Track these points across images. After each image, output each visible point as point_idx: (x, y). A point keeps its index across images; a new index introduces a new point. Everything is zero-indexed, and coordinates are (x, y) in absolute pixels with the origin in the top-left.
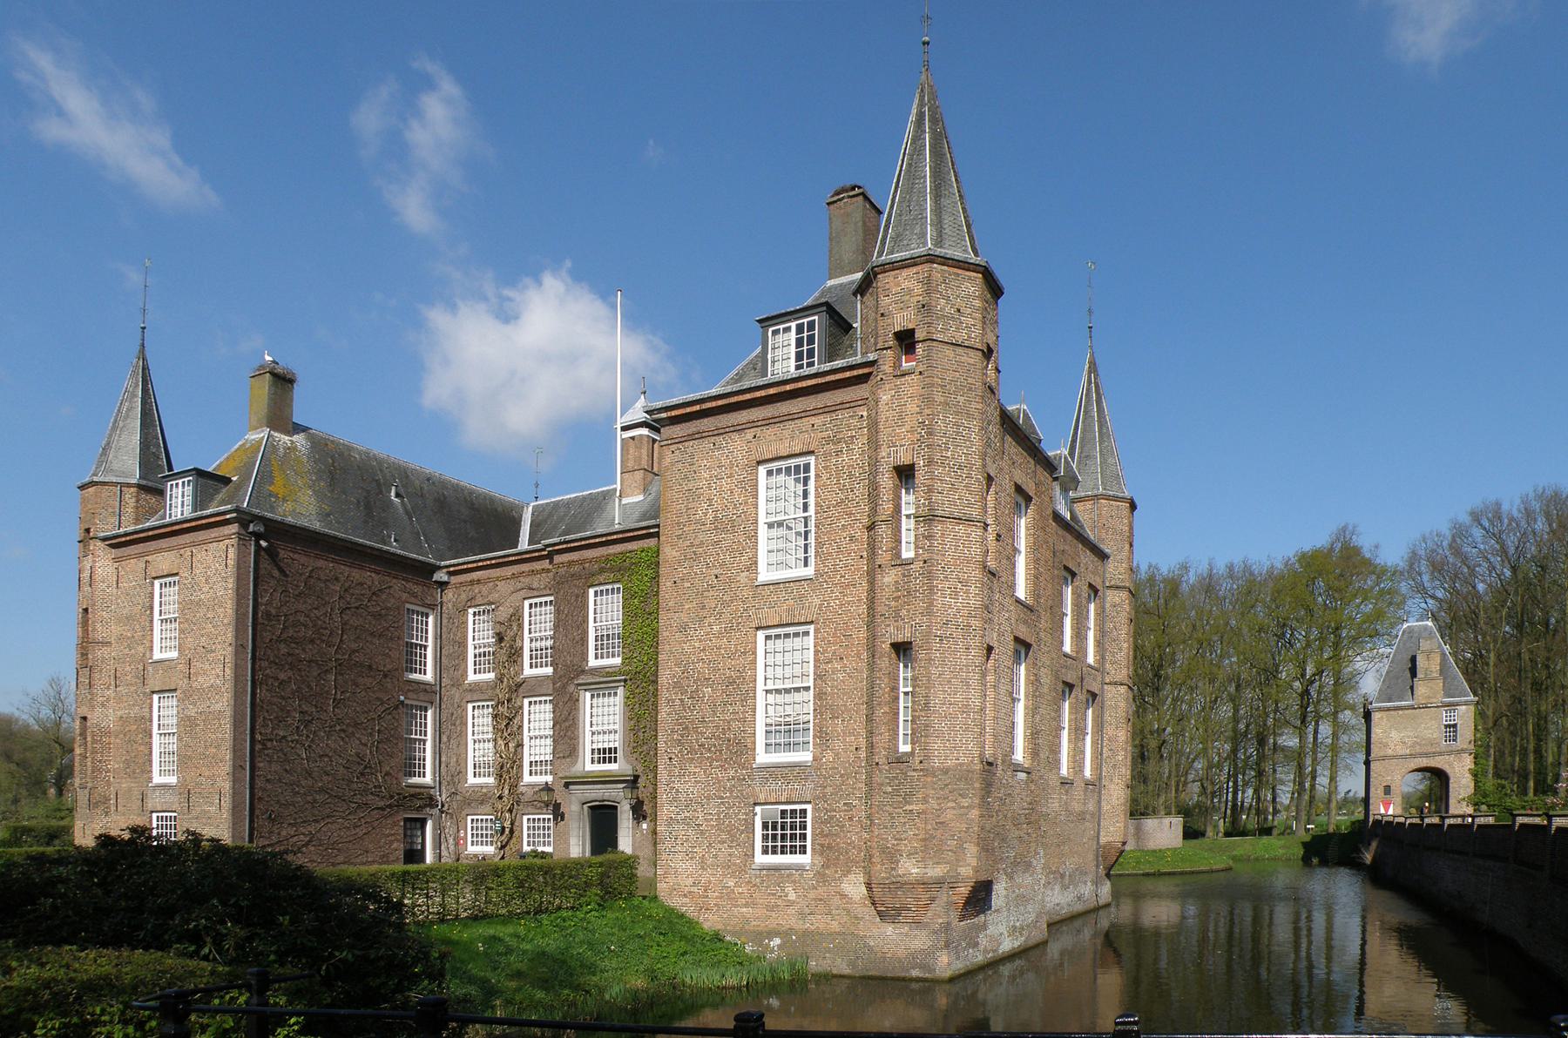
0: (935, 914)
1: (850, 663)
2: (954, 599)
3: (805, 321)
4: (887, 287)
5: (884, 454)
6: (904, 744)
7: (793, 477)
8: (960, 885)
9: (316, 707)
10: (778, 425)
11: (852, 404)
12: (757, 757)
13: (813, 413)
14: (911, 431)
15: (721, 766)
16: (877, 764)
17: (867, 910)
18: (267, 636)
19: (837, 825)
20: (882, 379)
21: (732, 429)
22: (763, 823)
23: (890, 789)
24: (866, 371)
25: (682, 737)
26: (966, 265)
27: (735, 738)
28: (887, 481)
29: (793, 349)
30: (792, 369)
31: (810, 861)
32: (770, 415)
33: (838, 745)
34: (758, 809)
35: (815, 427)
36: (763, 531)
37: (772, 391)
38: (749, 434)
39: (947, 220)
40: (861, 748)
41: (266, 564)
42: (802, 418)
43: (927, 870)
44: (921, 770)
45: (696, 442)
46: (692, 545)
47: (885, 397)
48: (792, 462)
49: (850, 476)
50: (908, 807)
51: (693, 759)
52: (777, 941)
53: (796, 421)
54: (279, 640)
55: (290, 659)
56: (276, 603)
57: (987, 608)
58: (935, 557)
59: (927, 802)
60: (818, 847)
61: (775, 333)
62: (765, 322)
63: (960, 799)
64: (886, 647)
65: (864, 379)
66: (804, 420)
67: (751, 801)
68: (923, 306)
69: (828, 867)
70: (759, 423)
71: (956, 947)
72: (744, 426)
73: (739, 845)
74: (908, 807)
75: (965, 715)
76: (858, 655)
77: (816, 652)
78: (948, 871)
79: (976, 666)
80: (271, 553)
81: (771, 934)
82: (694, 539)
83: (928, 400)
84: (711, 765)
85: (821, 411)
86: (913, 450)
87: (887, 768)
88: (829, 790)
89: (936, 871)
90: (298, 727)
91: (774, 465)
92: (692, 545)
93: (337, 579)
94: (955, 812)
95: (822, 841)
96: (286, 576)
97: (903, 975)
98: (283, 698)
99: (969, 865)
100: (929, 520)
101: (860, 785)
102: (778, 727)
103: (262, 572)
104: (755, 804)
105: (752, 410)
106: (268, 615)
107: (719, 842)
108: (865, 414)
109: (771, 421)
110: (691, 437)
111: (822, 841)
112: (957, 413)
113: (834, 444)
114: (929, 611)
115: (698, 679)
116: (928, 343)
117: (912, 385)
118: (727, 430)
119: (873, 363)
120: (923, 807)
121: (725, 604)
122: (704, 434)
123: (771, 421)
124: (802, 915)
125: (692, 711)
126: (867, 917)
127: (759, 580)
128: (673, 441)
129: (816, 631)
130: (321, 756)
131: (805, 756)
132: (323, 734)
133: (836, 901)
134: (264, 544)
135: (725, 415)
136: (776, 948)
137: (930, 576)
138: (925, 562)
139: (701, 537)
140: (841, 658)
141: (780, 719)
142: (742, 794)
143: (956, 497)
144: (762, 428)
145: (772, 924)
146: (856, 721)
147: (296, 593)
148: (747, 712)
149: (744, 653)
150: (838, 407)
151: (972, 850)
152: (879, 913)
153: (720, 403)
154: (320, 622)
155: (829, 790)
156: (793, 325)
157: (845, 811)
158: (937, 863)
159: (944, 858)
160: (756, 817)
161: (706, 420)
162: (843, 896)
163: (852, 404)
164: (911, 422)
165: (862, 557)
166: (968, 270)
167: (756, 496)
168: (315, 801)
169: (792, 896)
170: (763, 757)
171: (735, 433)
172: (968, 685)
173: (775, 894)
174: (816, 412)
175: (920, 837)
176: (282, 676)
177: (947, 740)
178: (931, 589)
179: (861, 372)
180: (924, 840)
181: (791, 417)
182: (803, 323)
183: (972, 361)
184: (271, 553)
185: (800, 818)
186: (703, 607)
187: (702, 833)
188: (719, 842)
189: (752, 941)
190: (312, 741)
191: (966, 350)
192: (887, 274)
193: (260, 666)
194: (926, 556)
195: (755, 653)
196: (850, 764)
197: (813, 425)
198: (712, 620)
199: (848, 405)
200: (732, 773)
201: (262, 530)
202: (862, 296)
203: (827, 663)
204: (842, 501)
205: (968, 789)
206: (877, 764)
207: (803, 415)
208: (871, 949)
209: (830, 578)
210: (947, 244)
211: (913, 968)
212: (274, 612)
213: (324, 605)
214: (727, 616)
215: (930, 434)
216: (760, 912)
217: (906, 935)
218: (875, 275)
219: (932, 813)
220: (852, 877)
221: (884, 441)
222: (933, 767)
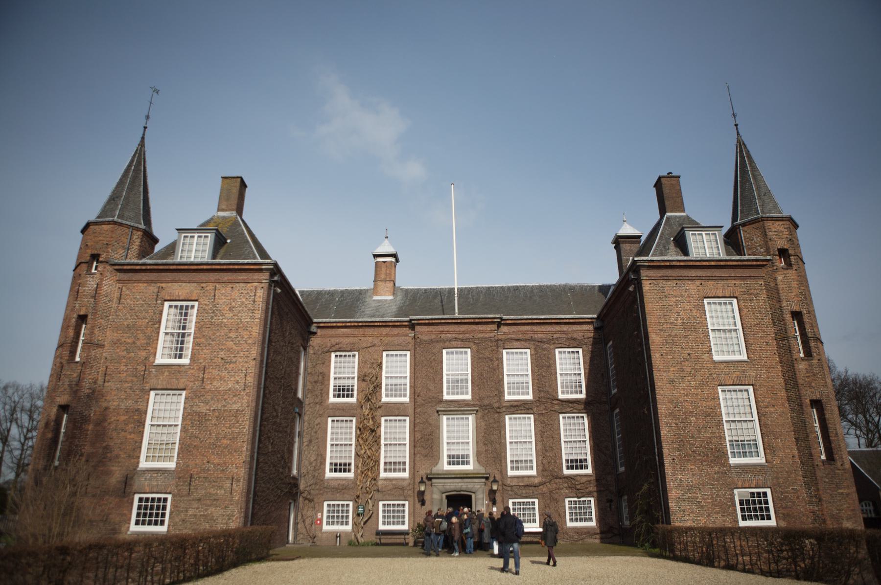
1: (780, 409)
5: (785, 305)
14: (796, 296)
16: (817, 465)
19: (790, 502)
22: (739, 500)
23: (827, 480)
24: (765, 263)
27: (716, 448)
32: (708, 275)
33: (781, 454)
34: (736, 491)
37: (713, 263)
38: (698, 283)
46: (670, 336)
51: (689, 460)
64: (808, 401)
73: (729, 515)
76: (783, 405)
88: (781, 480)
92: (670, 336)
101: (800, 478)
102: (743, 443)
107: (715, 513)
108: (763, 283)
113: (748, 295)
125: (684, 431)
131: (761, 460)
139: (675, 332)
157: (793, 493)
175: (851, 508)
179: (761, 263)
187: (702, 507)
194: (818, 357)
198: (689, 378)
200: (717, 469)
204: (758, 324)
214: (699, 378)
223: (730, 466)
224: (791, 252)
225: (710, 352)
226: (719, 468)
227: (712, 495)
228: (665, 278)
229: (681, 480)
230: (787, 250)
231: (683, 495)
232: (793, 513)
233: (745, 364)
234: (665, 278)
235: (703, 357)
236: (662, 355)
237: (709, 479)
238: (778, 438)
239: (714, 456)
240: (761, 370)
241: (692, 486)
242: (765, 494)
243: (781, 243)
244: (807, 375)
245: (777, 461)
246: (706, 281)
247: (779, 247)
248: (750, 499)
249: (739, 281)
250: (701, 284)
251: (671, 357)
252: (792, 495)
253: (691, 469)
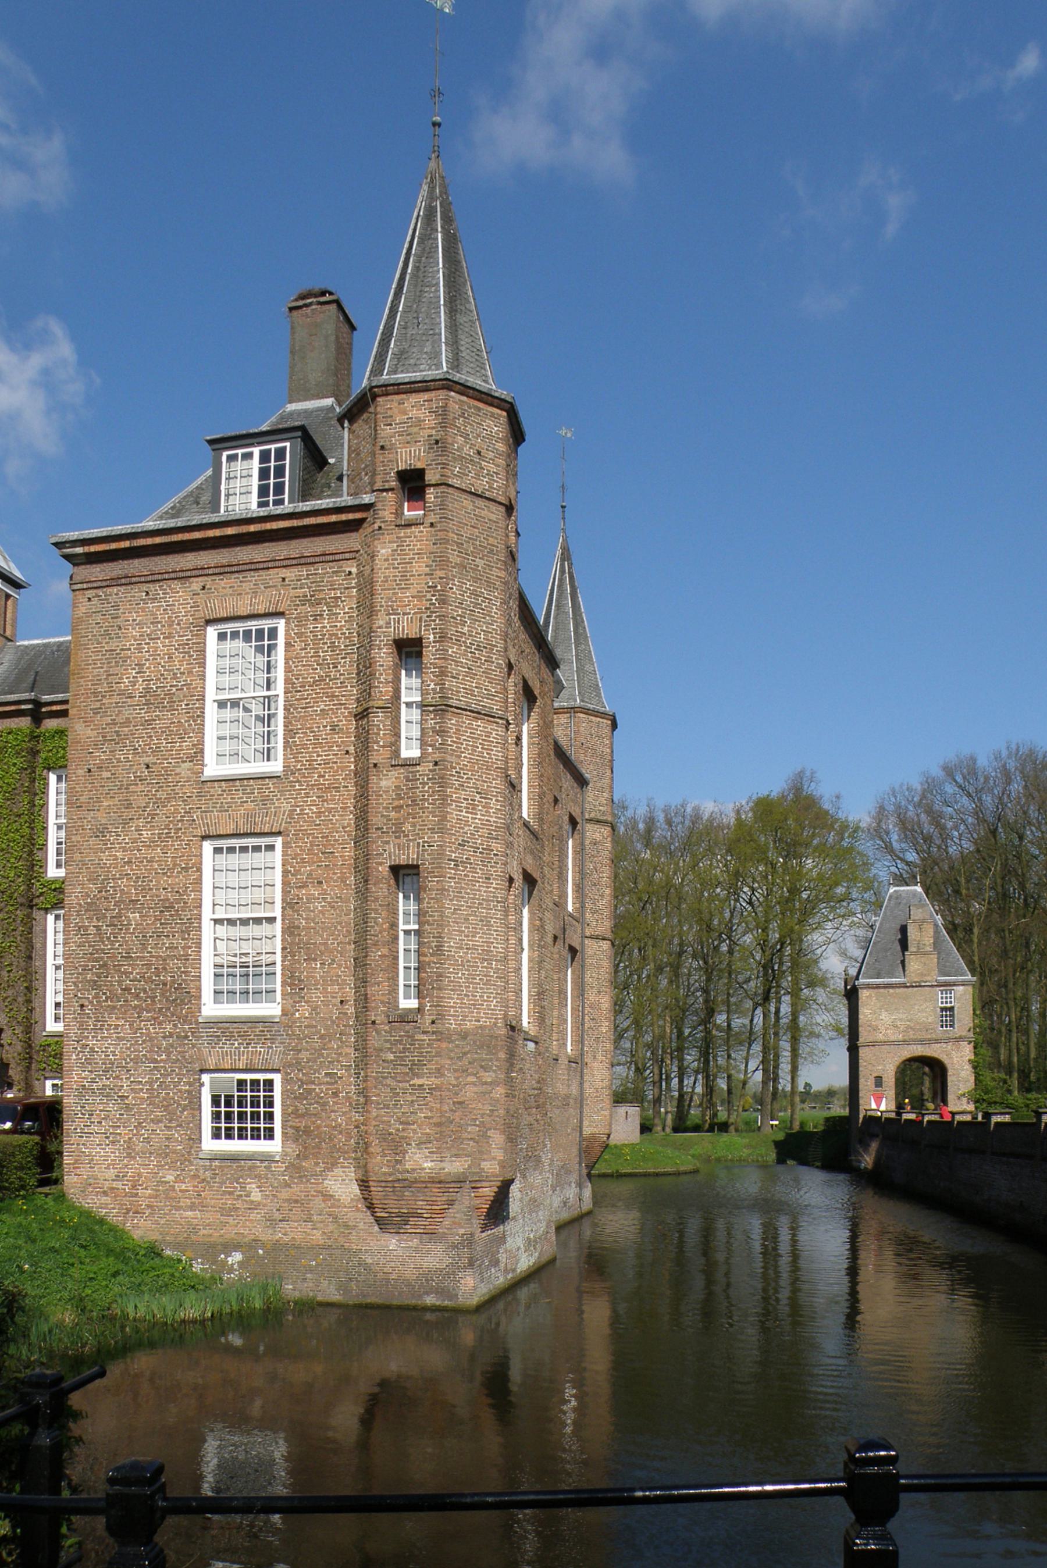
0: (454, 1223)
2: (471, 813)
3: (273, 447)
4: (389, 413)
5: (381, 623)
6: (405, 998)
7: (253, 644)
8: (484, 1184)
10: (237, 575)
11: (341, 557)
12: (203, 1007)
13: (284, 563)
14: (419, 597)
15: (155, 1019)
16: (374, 1022)
17: (360, 1215)
19: (317, 1103)
20: (380, 528)
21: (172, 575)
22: (213, 1096)
24: (358, 516)
25: (99, 977)
26: (490, 398)
28: (384, 657)
29: (255, 482)
30: (254, 506)
31: (279, 1149)
32: (225, 562)
33: (316, 996)
34: (206, 1078)
35: (287, 582)
36: (211, 711)
37: (230, 531)
38: (196, 584)
39: (464, 341)
40: (348, 1001)
42: (268, 568)
43: (443, 1165)
44: (434, 1033)
45: (122, 589)
46: (114, 723)
47: (383, 551)
48: (253, 625)
49: (333, 647)
50: (417, 1081)
51: (114, 1008)
52: (236, 1257)
53: (261, 573)
58: (449, 758)
59: (442, 1075)
60: (290, 1131)
61: (232, 458)
62: (218, 444)
63: (482, 1073)
64: (384, 870)
65: (354, 526)
66: (271, 571)
67: (197, 1067)
68: (437, 442)
69: (306, 1158)
70: (211, 571)
71: (480, 1266)
72: (189, 574)
73: (180, 1126)
74: (417, 1081)
75: (485, 964)
77: (285, 873)
78: (470, 1167)
79: (498, 902)
81: (229, 1247)
82: (117, 715)
83: (440, 561)
84: (139, 1017)
85: (294, 562)
86: (420, 621)
87: (387, 1028)
88: (304, 1055)
89: (455, 1167)
91: (229, 627)
94: (475, 1089)
95: (296, 1122)
97: (414, 1302)
99: (494, 1159)
100: (442, 710)
102: (230, 970)
104: (202, 1071)
105: (201, 553)
107: (152, 1120)
108: (354, 570)
109: (227, 569)
110: (115, 582)
111: (296, 1122)
112: (476, 580)
113: (312, 605)
114: (441, 828)
115: (121, 901)
116: (442, 489)
117: (419, 539)
118: (166, 576)
119: (367, 507)
120: (438, 1081)
121: (160, 803)
122: (134, 580)
123: (227, 569)
124: (271, 1222)
125: (112, 943)
126: (361, 1226)
127: (205, 774)
128: (90, 585)
129: (286, 845)
131: (272, 1009)
133: (318, 1203)
135: (164, 557)
136: (235, 1267)
137: (442, 782)
138: (436, 764)
139: (127, 713)
140: (320, 883)
141: (234, 959)
142: (184, 1057)
143: (474, 685)
144: (214, 577)
145: (230, 1232)
146: (340, 966)
148: (190, 947)
149: (186, 869)
150: (317, 559)
151: (497, 1138)
152: (379, 1221)
153: (158, 540)
155: (304, 1055)
156: (256, 451)
157: (328, 1083)
158: (456, 1156)
159: (464, 1149)
160: (203, 1089)
161: (136, 562)
162: (327, 1197)
163: (337, 557)
164: (418, 585)
165: (347, 752)
166: (491, 405)
167: (203, 665)
169: (256, 1196)
170: (210, 1009)
171: (176, 582)
173: (231, 1193)
174: (288, 563)
177: (466, 995)
178: (444, 798)
179: (351, 516)
180: (439, 1125)
181: (253, 567)
182: (270, 450)
183: (493, 517)
185: (264, 1091)
186: (129, 806)
187: (128, 1108)
188: (152, 1120)
189: (202, 1256)
191: (487, 503)
192: (390, 397)
194: (437, 756)
195: (199, 870)
196: (333, 1022)
197: (284, 579)
199: (331, 558)
202: (351, 422)
203: (300, 887)
204: (322, 679)
206: (374, 1022)
207: (270, 565)
208: (367, 1268)
209: (305, 777)
210: (465, 370)
211: (427, 1294)
215: (443, 602)
216: (210, 1217)
217: (417, 1250)
218: (374, 397)
219: (449, 1090)
220: (338, 1171)
221: (381, 606)
222: (448, 1029)
223: (197, 1023)
224: (431, 477)
225: (198, 754)
226: (175, 1025)
227: (151, 1082)
228: (123, 581)
229: (92, 1050)
230: (420, 473)
231: (93, 1081)
232: (318, 1127)
233: (270, 783)
234: (123, 581)
235: (178, 770)
236: (90, 771)
237: (151, 1051)
238: (315, 960)
239: (167, 1000)
240: (307, 795)
241: (113, 1064)
242: (269, 1083)
243: (408, 457)
244: (396, 803)
245: (303, 1011)
246: (217, 578)
247: (402, 467)
248: (236, 1094)
249: (295, 570)
250: (204, 588)
251: (109, 775)
252: (324, 1087)
253: (117, 1027)
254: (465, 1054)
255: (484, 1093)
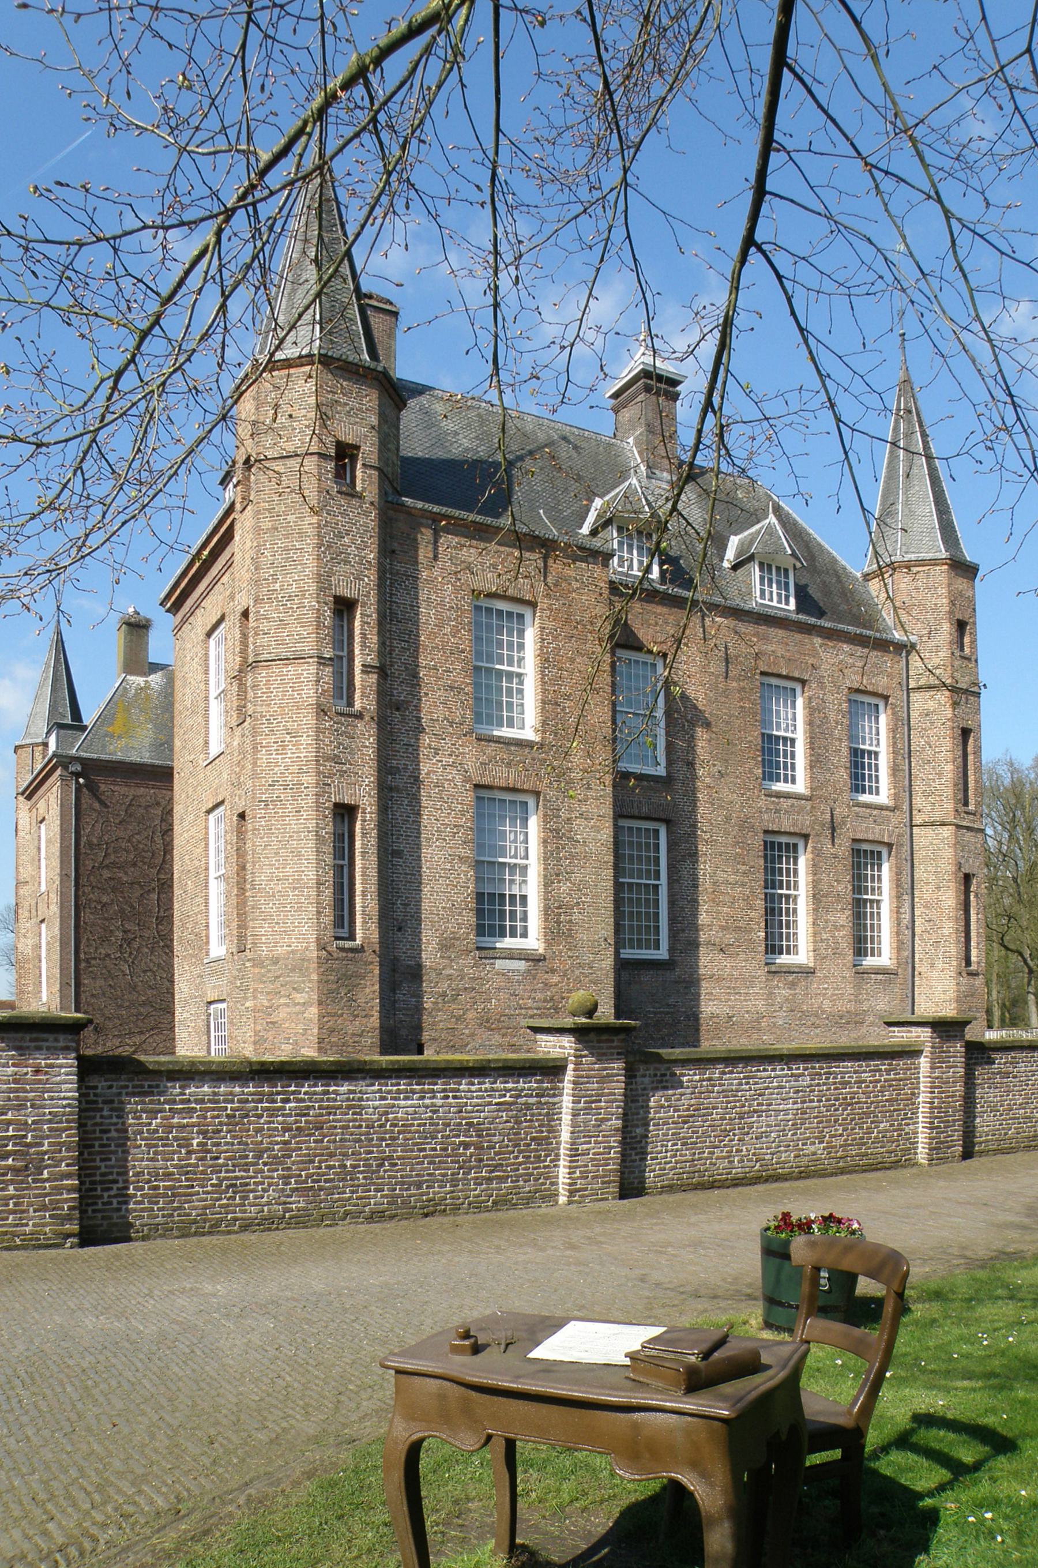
9: (139, 925)
18: (89, 864)
41: (87, 798)
54: (102, 866)
55: (112, 883)
56: (98, 832)
57: (336, 759)
58: (259, 709)
64: (235, 818)
79: (309, 832)
80: (92, 788)
90: (121, 946)
93: (158, 804)
94: (288, 1010)
96: (107, 806)
98: (106, 919)
103: (84, 806)
106: (90, 844)
130: (145, 972)
132: (147, 950)
134: (81, 780)
147: (117, 821)
154: (141, 846)
168: (140, 1014)
172: (299, 855)
176: (105, 899)
184: (92, 788)
190: (136, 957)
193: (84, 892)
201: (79, 769)
205: (303, 982)
212: (95, 841)
213: (145, 830)
254: (278, 977)
255: (297, 1014)
